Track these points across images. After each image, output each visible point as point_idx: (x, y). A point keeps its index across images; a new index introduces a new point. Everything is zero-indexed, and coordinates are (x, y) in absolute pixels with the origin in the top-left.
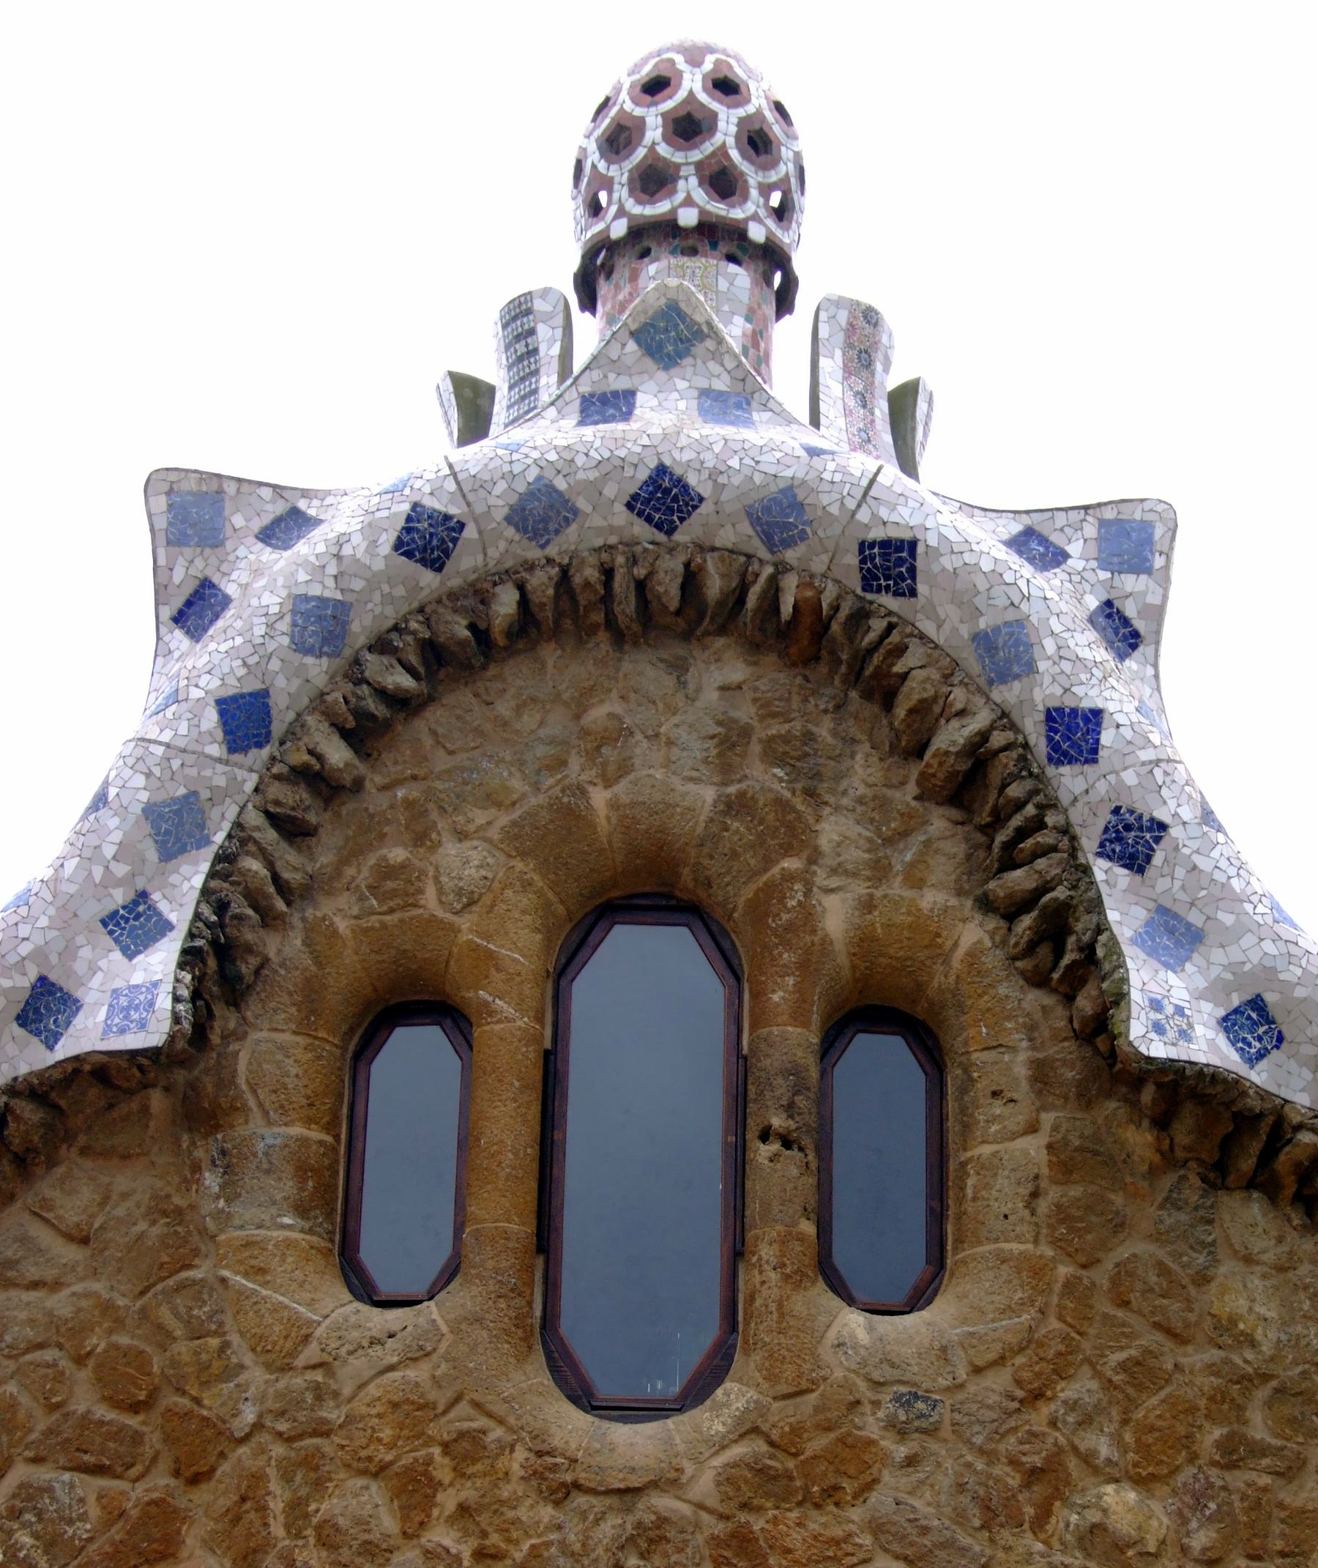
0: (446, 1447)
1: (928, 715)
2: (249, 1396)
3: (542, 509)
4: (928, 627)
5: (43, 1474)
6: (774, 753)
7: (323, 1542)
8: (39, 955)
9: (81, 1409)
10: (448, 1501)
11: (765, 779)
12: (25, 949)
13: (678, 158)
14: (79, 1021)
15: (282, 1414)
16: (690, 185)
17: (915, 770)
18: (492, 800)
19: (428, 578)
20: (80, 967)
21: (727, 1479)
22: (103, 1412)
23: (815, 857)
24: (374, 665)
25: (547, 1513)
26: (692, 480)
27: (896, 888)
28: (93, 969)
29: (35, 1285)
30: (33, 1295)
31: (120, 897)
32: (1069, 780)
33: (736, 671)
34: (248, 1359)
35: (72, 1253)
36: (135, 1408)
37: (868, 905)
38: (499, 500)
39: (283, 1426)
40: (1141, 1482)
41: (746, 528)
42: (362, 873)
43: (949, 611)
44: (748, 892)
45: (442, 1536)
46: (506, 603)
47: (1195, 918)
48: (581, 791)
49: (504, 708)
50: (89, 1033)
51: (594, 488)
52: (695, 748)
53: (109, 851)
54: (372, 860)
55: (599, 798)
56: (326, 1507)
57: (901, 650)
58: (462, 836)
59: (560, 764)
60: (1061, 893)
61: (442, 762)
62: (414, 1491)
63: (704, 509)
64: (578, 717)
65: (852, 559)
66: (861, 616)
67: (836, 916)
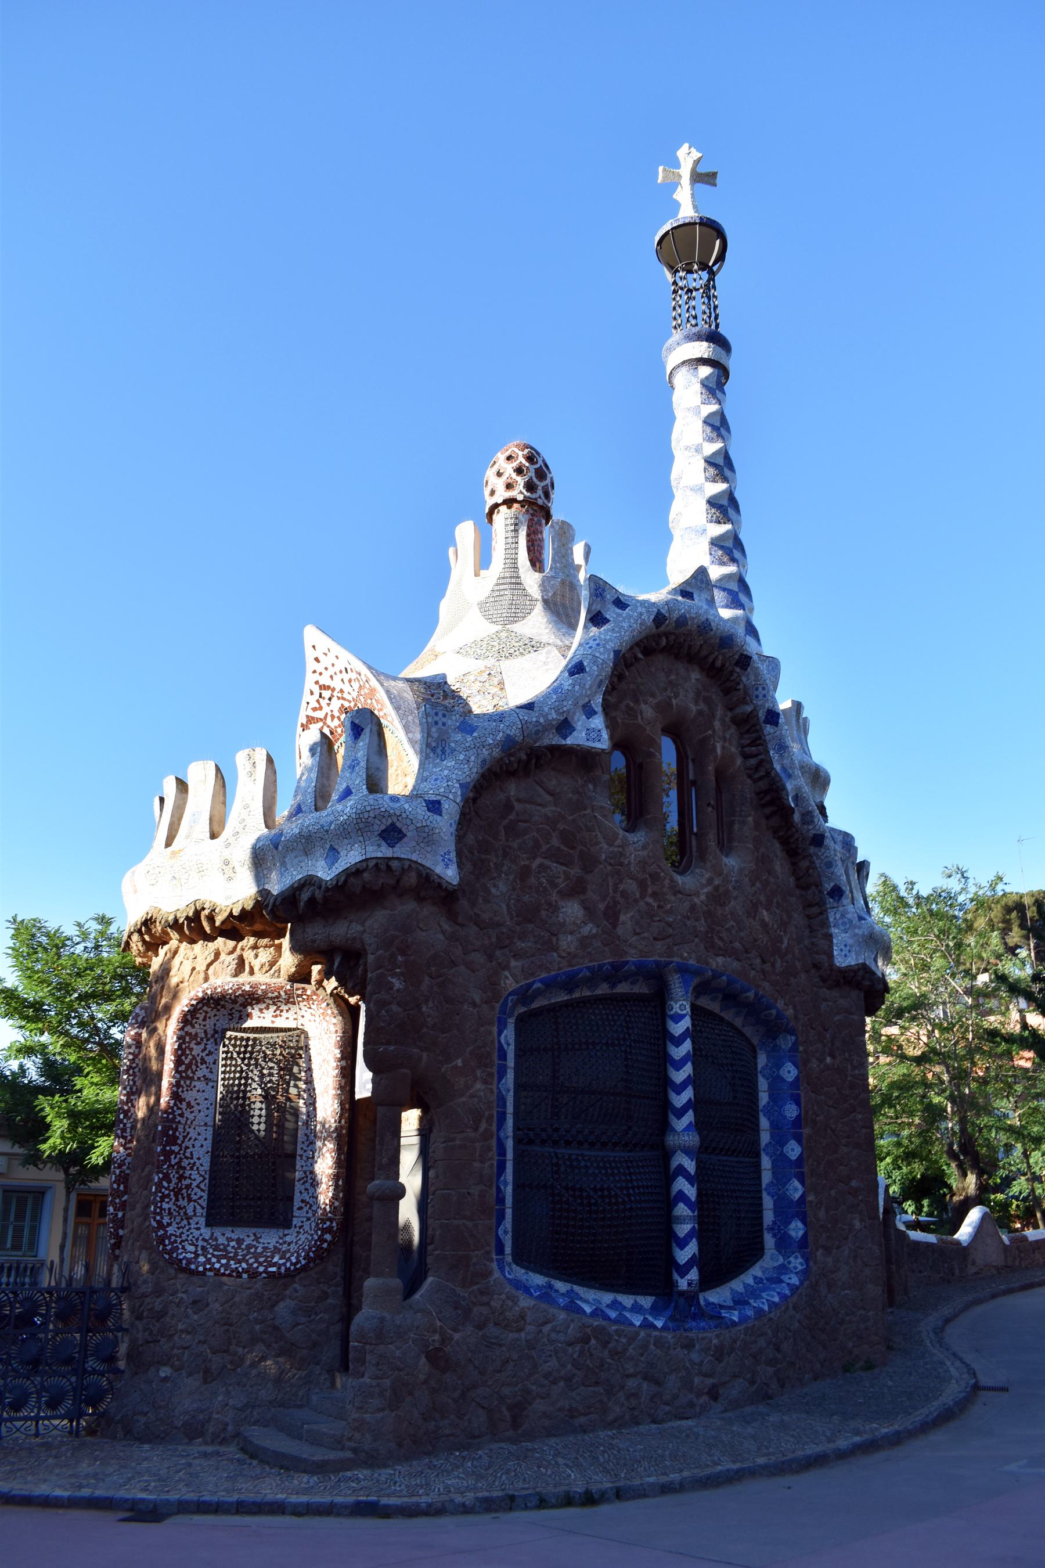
0: (650, 876)
1: (744, 701)
2: (604, 850)
3: (682, 621)
4: (744, 679)
5: (547, 862)
6: (707, 701)
7: (622, 896)
8: (568, 711)
9: (557, 845)
10: (650, 891)
11: (702, 706)
12: (565, 709)
13: (538, 483)
14: (575, 733)
15: (611, 858)
16: (540, 492)
17: (730, 714)
18: (653, 695)
19: (654, 630)
20: (576, 718)
21: (708, 895)
22: (562, 847)
23: (714, 731)
24: (637, 650)
25: (673, 898)
26: (712, 624)
27: (727, 744)
28: (579, 720)
29: (540, 805)
30: (539, 808)
31: (587, 700)
32: (769, 729)
33: (698, 677)
34: (602, 840)
35: (549, 798)
36: (573, 848)
37: (723, 748)
38: (675, 615)
39: (612, 861)
40: (767, 910)
41: (717, 641)
42: (622, 706)
43: (752, 677)
44: (701, 737)
45: (650, 900)
46: (664, 642)
47: (791, 771)
48: (670, 698)
49: (653, 669)
50: (578, 738)
51: (693, 619)
52: (691, 695)
53: (587, 686)
54: (624, 703)
55: (674, 702)
56: (622, 887)
57: (738, 684)
58: (646, 703)
59: (666, 689)
60: (762, 757)
61: (639, 680)
62: (642, 885)
63: (712, 633)
64: (668, 677)
65: (737, 657)
66: (732, 672)
67: (719, 751)
